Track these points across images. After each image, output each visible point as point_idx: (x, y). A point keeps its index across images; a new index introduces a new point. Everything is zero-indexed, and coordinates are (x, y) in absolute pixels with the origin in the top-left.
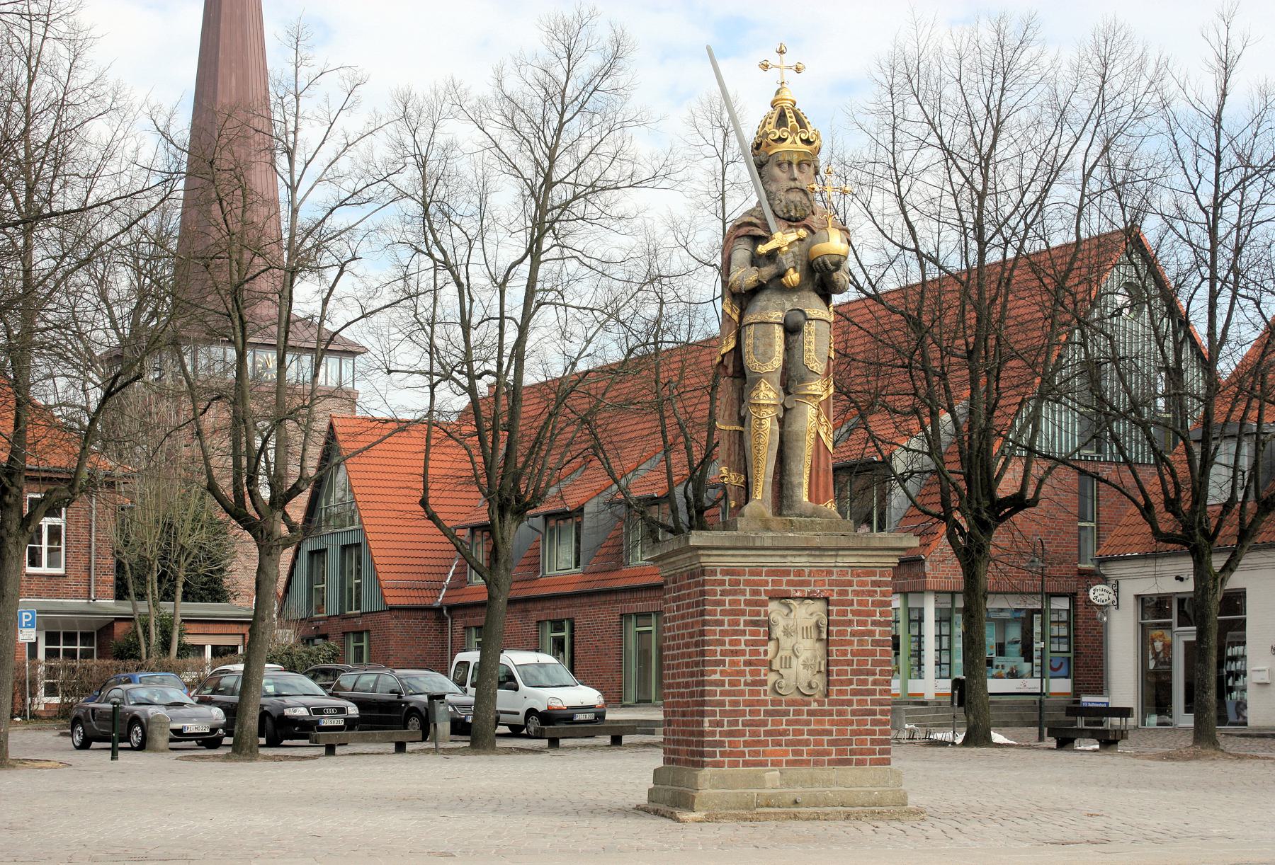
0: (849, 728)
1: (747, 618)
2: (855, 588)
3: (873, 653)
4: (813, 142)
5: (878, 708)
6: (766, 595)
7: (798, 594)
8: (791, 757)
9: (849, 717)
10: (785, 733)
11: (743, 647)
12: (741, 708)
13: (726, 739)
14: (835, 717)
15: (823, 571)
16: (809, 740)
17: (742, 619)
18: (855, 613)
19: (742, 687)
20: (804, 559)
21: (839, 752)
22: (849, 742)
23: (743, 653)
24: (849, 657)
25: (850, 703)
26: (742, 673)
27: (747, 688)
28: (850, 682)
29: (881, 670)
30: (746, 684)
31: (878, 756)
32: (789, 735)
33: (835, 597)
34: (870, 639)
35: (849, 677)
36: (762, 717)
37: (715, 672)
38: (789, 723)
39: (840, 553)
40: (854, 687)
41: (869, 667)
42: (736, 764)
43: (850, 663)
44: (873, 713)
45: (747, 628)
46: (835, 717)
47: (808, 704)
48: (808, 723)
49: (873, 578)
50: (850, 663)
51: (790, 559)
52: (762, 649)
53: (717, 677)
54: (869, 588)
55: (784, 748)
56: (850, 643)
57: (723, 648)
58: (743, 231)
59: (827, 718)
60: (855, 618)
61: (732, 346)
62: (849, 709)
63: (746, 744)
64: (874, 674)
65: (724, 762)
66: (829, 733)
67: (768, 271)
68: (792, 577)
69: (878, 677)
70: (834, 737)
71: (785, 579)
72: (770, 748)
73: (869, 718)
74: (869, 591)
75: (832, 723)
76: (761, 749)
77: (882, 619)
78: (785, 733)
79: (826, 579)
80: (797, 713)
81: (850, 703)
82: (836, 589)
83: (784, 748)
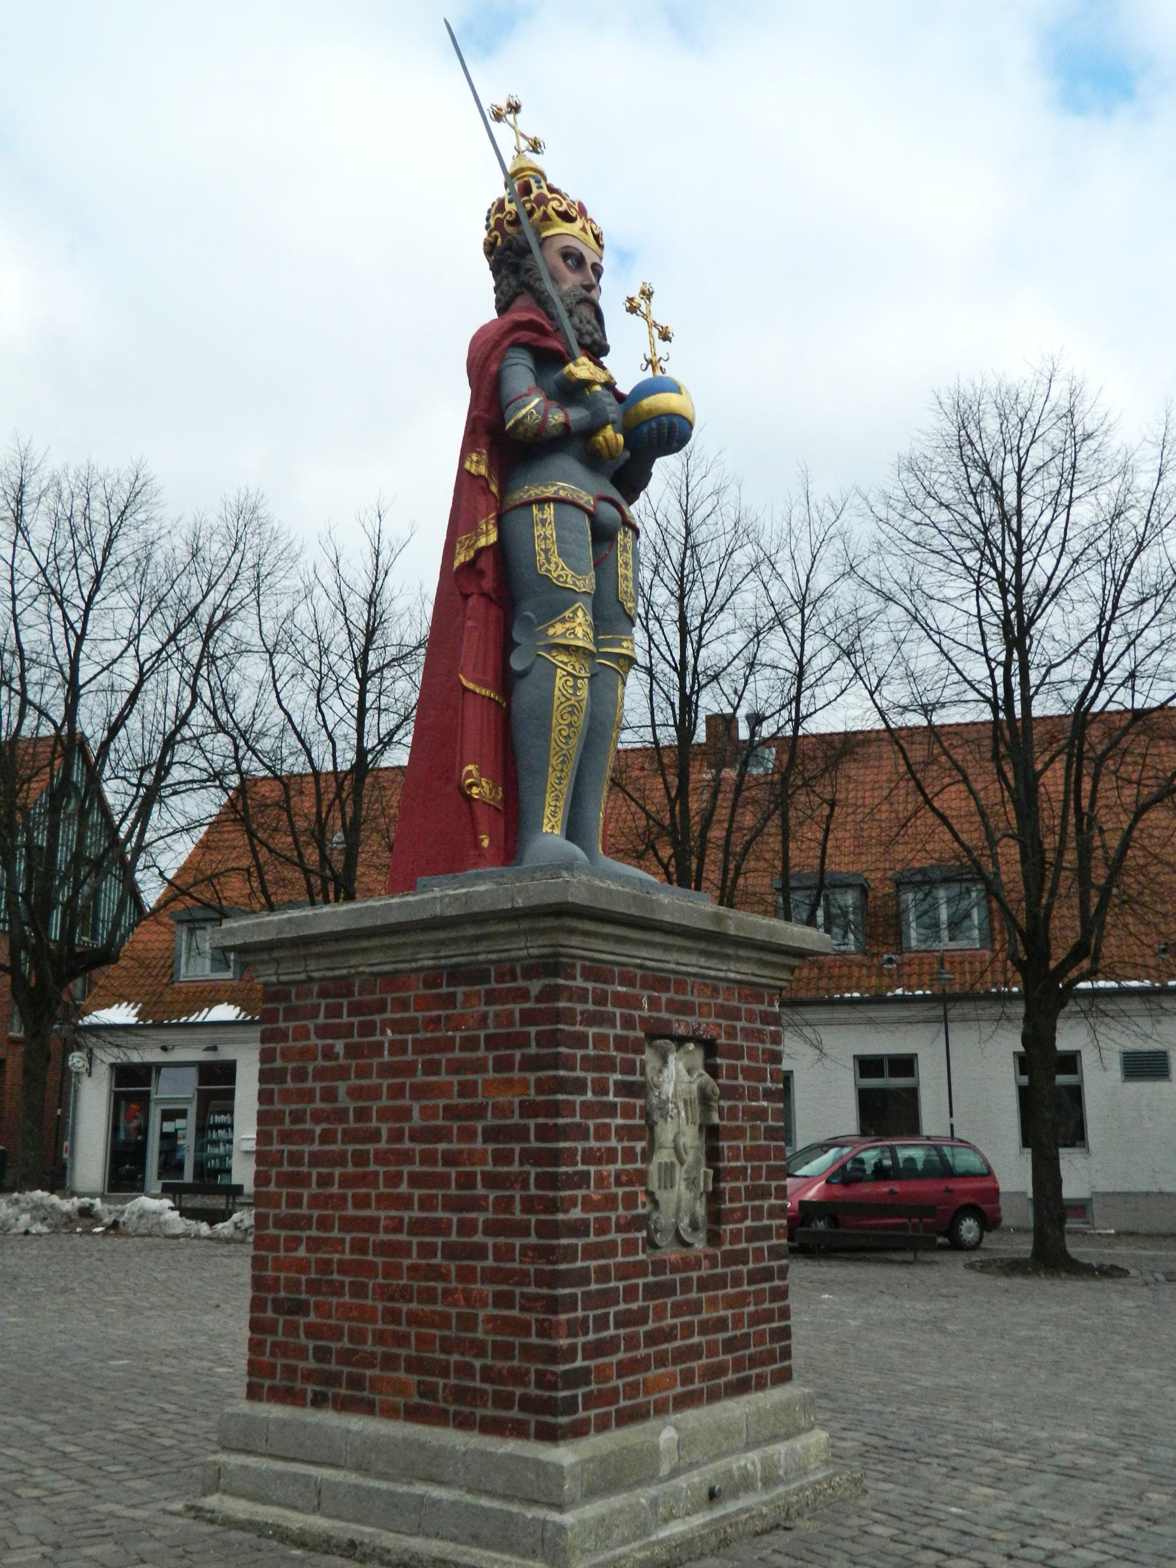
7: (681, 1031)
20: (693, 959)
27: (619, 1237)
37: (573, 1202)
51: (675, 956)
53: (576, 1213)
58: (525, 336)
61: (493, 538)
67: (577, 415)
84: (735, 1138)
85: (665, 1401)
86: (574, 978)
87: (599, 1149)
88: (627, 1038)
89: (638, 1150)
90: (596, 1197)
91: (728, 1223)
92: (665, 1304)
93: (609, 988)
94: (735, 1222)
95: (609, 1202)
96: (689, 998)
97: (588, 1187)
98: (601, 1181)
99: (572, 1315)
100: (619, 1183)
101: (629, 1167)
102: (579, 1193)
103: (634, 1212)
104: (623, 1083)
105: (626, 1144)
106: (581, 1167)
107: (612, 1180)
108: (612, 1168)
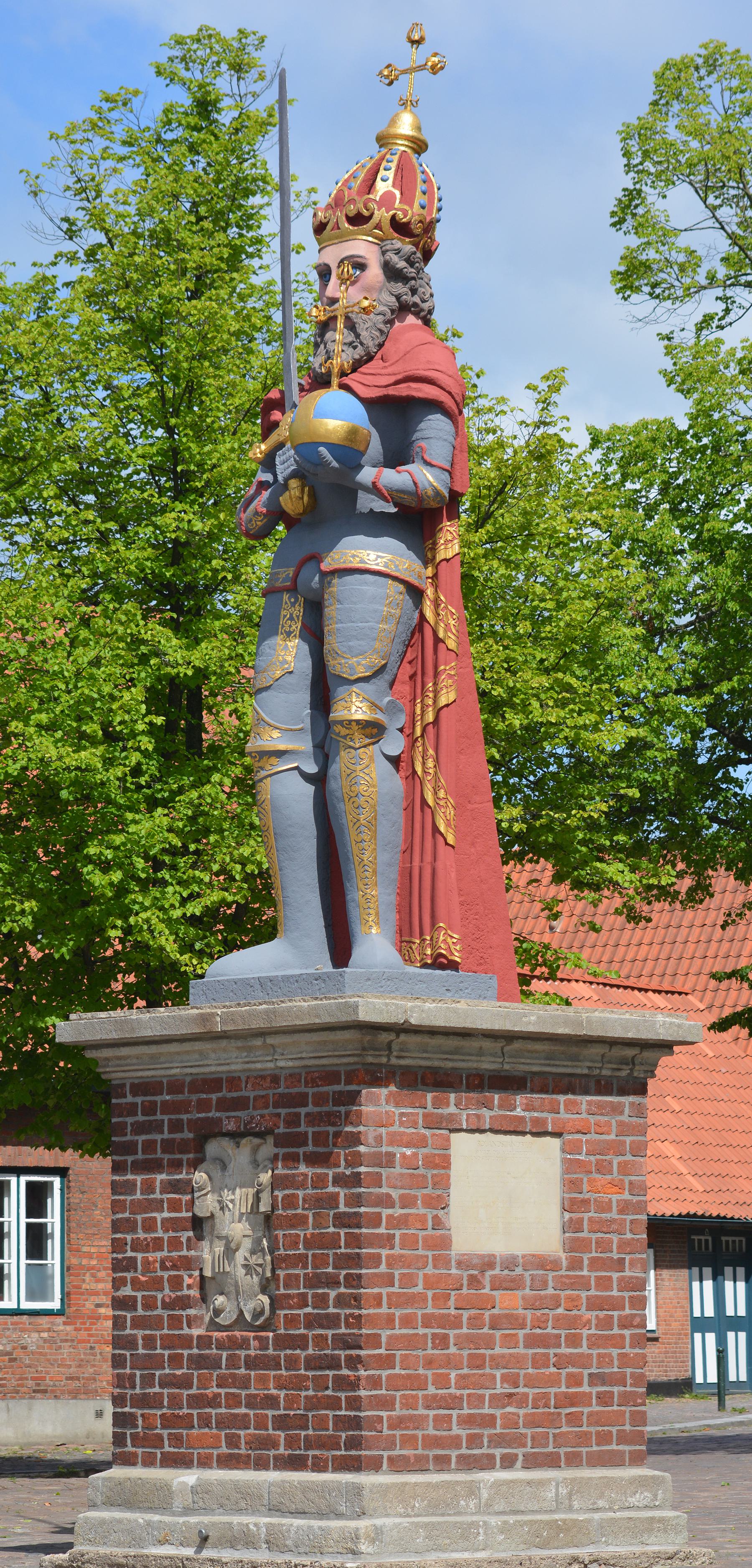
0: (303, 1394)
2: (311, 1108)
5: (342, 1354)
6: (190, 1131)
7: (231, 1126)
8: (224, 1450)
9: (302, 1372)
10: (214, 1402)
12: (158, 1351)
15: (263, 1077)
16: (246, 1415)
21: (291, 1442)
27: (165, 1314)
29: (347, 1276)
30: (165, 1306)
33: (281, 1130)
34: (332, 1213)
35: (302, 1290)
39: (270, 1040)
41: (330, 1270)
42: (149, 1462)
43: (302, 1260)
46: (283, 1372)
48: (245, 1383)
49: (337, 1088)
50: (302, 1260)
54: (330, 1108)
56: (301, 1221)
59: (273, 1373)
62: (303, 1354)
64: (337, 1284)
66: (271, 1402)
68: (224, 1093)
69: (342, 1290)
73: (331, 1373)
74: (329, 1114)
76: (185, 1432)
78: (214, 1402)
79: (271, 1092)
80: (233, 1362)
82: (283, 1111)
83: (214, 1431)
84: (293, 1226)
85: (209, 1457)
86: (125, 1096)
89: (184, 1240)
90: (143, 1279)
91: (283, 1308)
93: (158, 1098)
94: (291, 1308)
95: (157, 1284)
96: (243, 1093)
97: (136, 1271)
99: (122, 1371)
100: (164, 1268)
102: (129, 1275)
103: (179, 1293)
104: (170, 1182)
105: (171, 1234)
106: (130, 1254)
107: (158, 1265)
108: (159, 1255)
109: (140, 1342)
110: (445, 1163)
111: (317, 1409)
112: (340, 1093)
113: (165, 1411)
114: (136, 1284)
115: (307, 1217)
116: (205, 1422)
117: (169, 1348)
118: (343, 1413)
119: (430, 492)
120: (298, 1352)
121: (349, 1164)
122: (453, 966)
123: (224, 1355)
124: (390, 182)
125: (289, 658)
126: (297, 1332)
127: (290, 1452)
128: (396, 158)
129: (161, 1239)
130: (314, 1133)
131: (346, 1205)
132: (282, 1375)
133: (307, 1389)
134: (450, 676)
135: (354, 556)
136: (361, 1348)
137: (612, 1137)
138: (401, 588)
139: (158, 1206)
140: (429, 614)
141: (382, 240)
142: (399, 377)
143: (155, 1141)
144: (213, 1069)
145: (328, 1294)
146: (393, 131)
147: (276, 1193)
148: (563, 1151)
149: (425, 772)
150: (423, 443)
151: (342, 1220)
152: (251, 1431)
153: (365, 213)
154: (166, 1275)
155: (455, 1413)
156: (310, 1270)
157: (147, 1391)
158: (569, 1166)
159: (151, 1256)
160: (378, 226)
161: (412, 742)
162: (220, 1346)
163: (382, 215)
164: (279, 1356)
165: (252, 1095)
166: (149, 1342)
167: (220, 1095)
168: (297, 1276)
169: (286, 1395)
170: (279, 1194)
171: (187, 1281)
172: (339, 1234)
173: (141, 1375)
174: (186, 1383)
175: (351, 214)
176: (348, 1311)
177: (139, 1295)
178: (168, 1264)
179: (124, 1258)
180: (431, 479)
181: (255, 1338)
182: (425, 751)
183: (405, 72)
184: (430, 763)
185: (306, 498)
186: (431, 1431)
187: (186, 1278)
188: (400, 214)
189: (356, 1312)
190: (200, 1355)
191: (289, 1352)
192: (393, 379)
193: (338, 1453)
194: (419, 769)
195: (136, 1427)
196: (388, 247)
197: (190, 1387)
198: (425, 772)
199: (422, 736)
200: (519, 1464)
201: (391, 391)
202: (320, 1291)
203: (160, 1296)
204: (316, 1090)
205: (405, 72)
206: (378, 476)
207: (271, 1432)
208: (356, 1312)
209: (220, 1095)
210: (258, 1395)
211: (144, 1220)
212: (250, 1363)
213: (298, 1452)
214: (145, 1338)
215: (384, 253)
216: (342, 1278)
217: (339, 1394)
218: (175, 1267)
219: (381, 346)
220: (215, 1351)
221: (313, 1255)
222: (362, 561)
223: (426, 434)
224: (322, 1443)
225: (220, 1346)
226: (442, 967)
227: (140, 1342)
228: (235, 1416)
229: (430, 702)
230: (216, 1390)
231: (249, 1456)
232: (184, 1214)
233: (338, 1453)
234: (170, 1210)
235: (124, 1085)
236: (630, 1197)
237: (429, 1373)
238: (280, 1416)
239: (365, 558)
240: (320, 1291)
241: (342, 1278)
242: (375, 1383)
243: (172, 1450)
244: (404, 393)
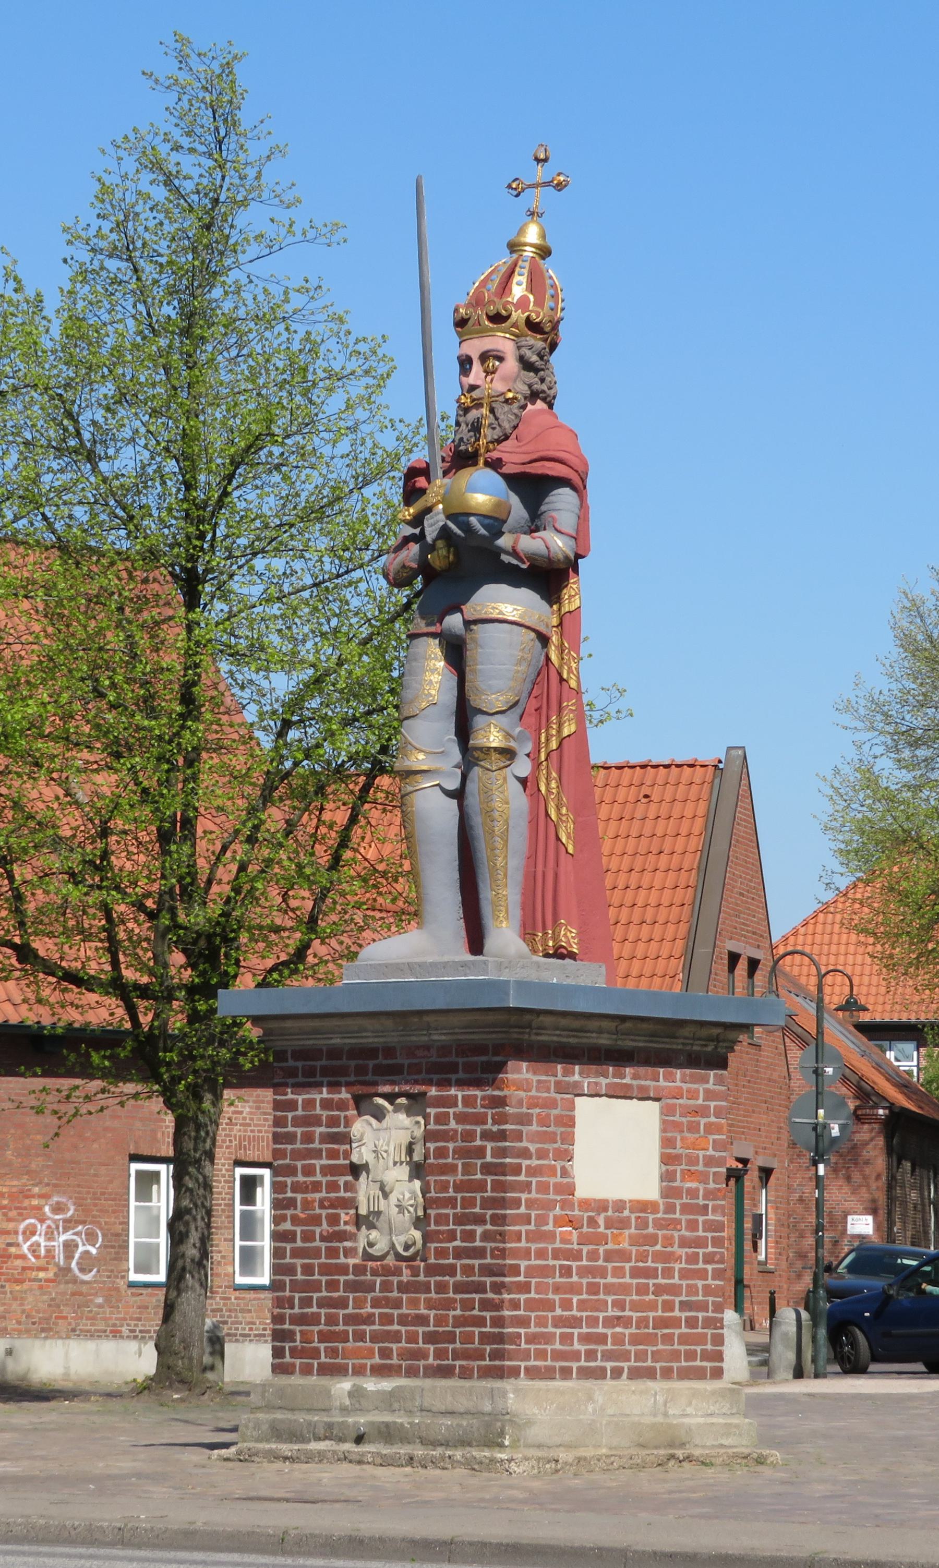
0: (452, 1313)
1: (323, 1129)
3: (481, 1186)
4: (508, 317)
5: (488, 1280)
8: (377, 1360)
9: (451, 1295)
10: (369, 1319)
11: (318, 1177)
13: (298, 1328)
14: (433, 1295)
16: (399, 1332)
17: (319, 1130)
18: (461, 1118)
19: (317, 1243)
21: (439, 1355)
22: (451, 1338)
23: (316, 1187)
24: (451, 1193)
25: (451, 1270)
26: (316, 1220)
27: (323, 1245)
28: (452, 1236)
29: (492, 1216)
30: (323, 1239)
31: (487, 1362)
32: (373, 1323)
35: (451, 1227)
36: (341, 1293)
38: (376, 1303)
40: (457, 1243)
41: (477, 1210)
42: (307, 1371)
43: (452, 1202)
44: (480, 1288)
45: (324, 1146)
46: (433, 1295)
47: (397, 1272)
48: (397, 1304)
50: (452, 1202)
52: (342, 1180)
55: (368, 1344)
56: (452, 1169)
57: (295, 1179)
59: (423, 1296)
60: (460, 1128)
63: (324, 1337)
65: (294, 1365)
66: (422, 1320)
69: (489, 1227)
70: (432, 1328)
71: (371, 1064)
72: (350, 1344)
73: (477, 1296)
75: (430, 1305)
77: (495, 1128)
78: (369, 1319)
80: (386, 1287)
81: (451, 1270)
83: (368, 1344)
84: (443, 1173)
85: (364, 1366)
86: (287, 1061)
87: (305, 1182)
88: (333, 1099)
89: (341, 1184)
90: (302, 1216)
91: (433, 1242)
92: (366, 1298)
93: (318, 1064)
94: (441, 1242)
95: (316, 1220)
97: (295, 1209)
98: (307, 1205)
100: (322, 1206)
101: (332, 1195)
102: (289, 1213)
103: (336, 1228)
104: (329, 1134)
105: (329, 1178)
106: (289, 1195)
107: (317, 1204)
108: (317, 1196)
109: (299, 1270)
110: (570, 1122)
111: (464, 1326)
112: (488, 1063)
113: (321, 1327)
114: (295, 1220)
115: (457, 1166)
116: (360, 1336)
117: (327, 1275)
118: (488, 1329)
119: (561, 556)
120: (447, 1278)
121: (495, 1122)
122: (572, 956)
123: (379, 1280)
124: (524, 286)
125: (433, 692)
126: (447, 1262)
127: (439, 1362)
128: (527, 265)
129: (320, 1183)
130: (463, 1096)
131: (492, 1157)
132: (431, 1298)
133: (455, 1309)
134: (572, 711)
135: (493, 608)
136: (505, 1276)
137: (700, 1102)
138: (533, 635)
139: (317, 1154)
140: (554, 657)
141: (517, 336)
142: (535, 456)
143: (315, 1100)
144: (371, 1040)
145: (475, 1231)
146: (523, 240)
147: (428, 1145)
148: (662, 1113)
149: (549, 791)
150: (554, 514)
151: (488, 1169)
152: (403, 1344)
153: (504, 313)
154: (324, 1213)
155: (576, 1331)
156: (459, 1210)
157: (305, 1310)
158: (666, 1126)
159: (310, 1196)
160: (515, 325)
161: (537, 765)
162: (375, 1273)
163: (518, 316)
164: (429, 1282)
165: (406, 1062)
166: (308, 1269)
167: (376, 1062)
168: (447, 1215)
169: (436, 1315)
170: (431, 1146)
171: (344, 1217)
172: (486, 1181)
173: (300, 1298)
174: (343, 1304)
175: (491, 314)
176: (493, 1245)
177: (298, 1230)
178: (326, 1204)
179: (284, 1199)
180: (560, 544)
181: (407, 1267)
182: (549, 773)
183: (530, 186)
184: (553, 784)
185: (451, 557)
186: (558, 1346)
187: (343, 1215)
188: (534, 316)
189: (501, 1245)
190: (355, 1281)
191: (438, 1278)
192: (527, 458)
193: (483, 1363)
194: (543, 789)
195: (295, 1341)
196: (524, 343)
197: (346, 1307)
198: (549, 791)
199: (546, 760)
200: (625, 1375)
201: (528, 469)
202: (468, 1227)
203: (318, 1230)
204: (465, 1059)
205: (530, 186)
206: (516, 541)
207: (421, 1345)
208: (501, 1245)
209: (376, 1062)
210: (409, 1315)
211: (303, 1166)
212: (403, 1288)
213: (446, 1362)
214: (303, 1266)
215: (519, 348)
216: (488, 1217)
217: (484, 1314)
218: (332, 1206)
219: (515, 427)
220: (369, 1277)
221: (462, 1198)
222: (501, 613)
223: (558, 506)
224: (466, 1355)
225: (375, 1273)
226: (562, 957)
227: (299, 1270)
228: (388, 1332)
229: (554, 732)
230: (369, 1310)
231: (401, 1366)
232: (342, 1162)
233: (483, 1363)
234: (328, 1158)
235: (286, 1052)
236: (713, 1153)
237: (557, 1297)
238: (429, 1332)
239: (504, 610)
240: (468, 1227)
241: (488, 1217)
242: (515, 1305)
243: (328, 1360)
244: (540, 472)
